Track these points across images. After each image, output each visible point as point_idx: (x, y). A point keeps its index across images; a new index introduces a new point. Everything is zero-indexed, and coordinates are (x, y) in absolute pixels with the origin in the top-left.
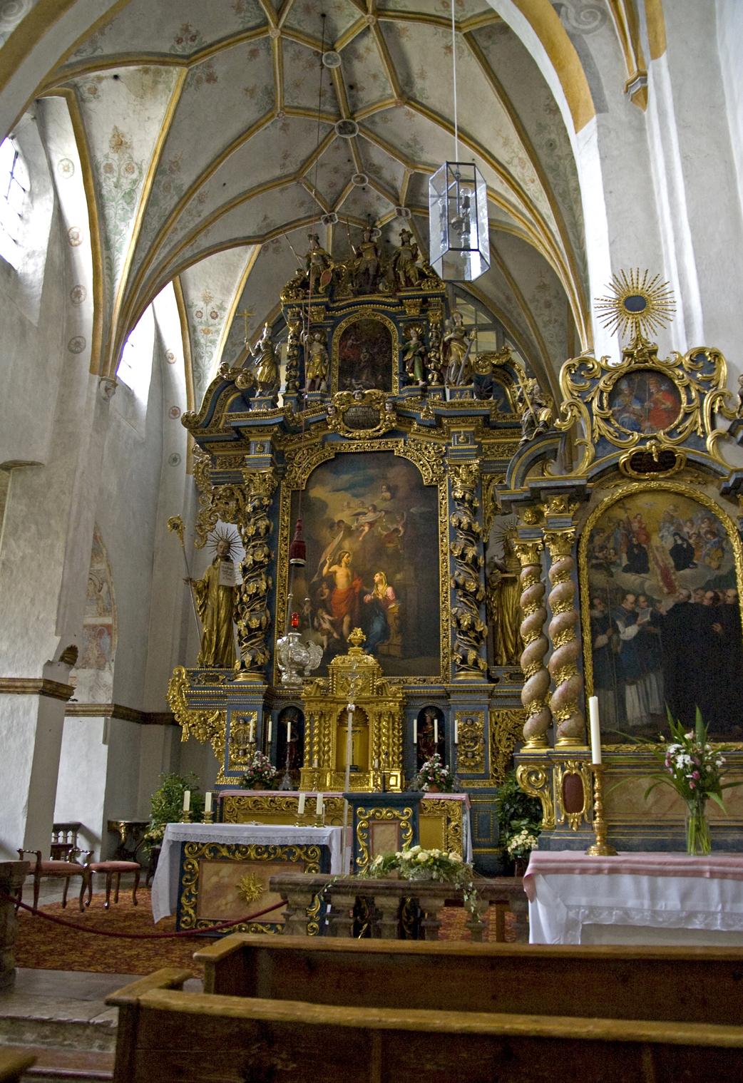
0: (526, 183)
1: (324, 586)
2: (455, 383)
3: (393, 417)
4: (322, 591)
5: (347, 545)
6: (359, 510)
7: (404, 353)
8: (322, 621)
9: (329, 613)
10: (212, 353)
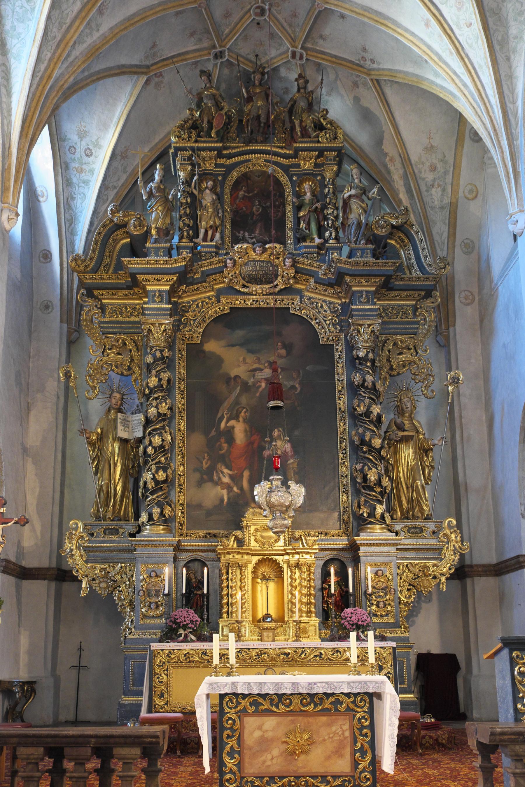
0: (460, 28)
1: (222, 440)
2: (355, 242)
3: (292, 272)
4: (220, 445)
6: (256, 366)
7: (298, 208)
8: (221, 475)
10: (84, 194)
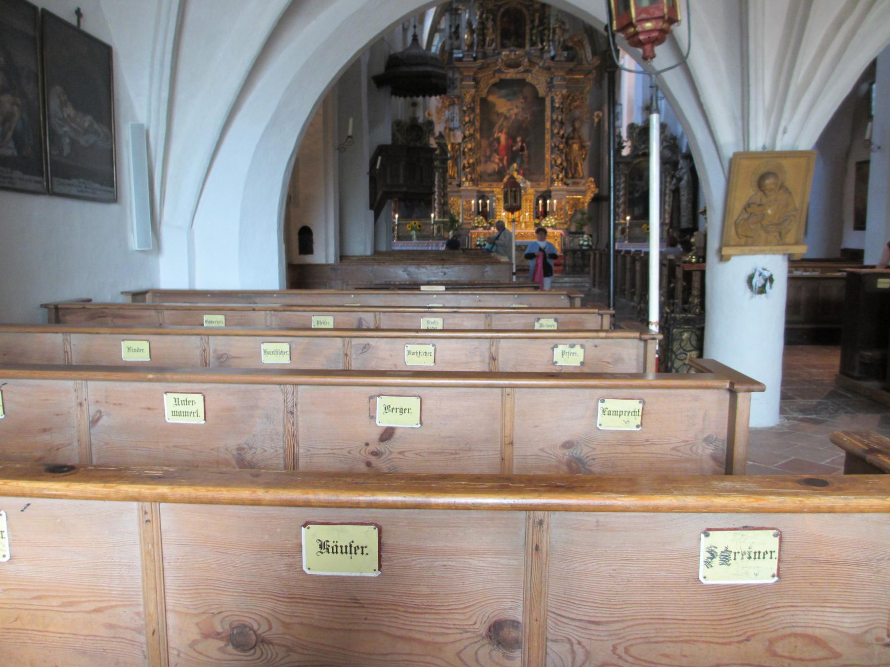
5: (505, 124)
6: (510, 107)
9: (498, 154)
